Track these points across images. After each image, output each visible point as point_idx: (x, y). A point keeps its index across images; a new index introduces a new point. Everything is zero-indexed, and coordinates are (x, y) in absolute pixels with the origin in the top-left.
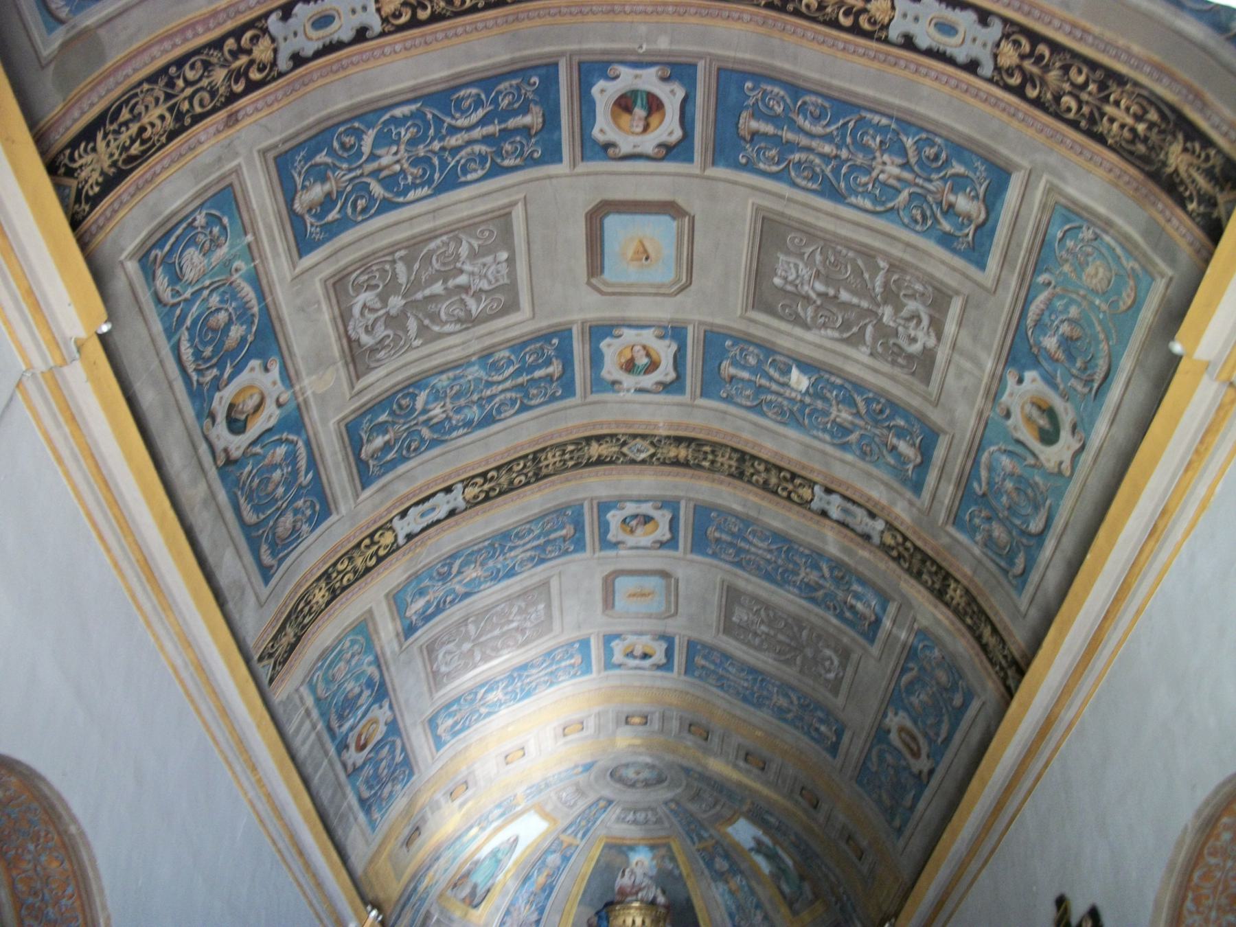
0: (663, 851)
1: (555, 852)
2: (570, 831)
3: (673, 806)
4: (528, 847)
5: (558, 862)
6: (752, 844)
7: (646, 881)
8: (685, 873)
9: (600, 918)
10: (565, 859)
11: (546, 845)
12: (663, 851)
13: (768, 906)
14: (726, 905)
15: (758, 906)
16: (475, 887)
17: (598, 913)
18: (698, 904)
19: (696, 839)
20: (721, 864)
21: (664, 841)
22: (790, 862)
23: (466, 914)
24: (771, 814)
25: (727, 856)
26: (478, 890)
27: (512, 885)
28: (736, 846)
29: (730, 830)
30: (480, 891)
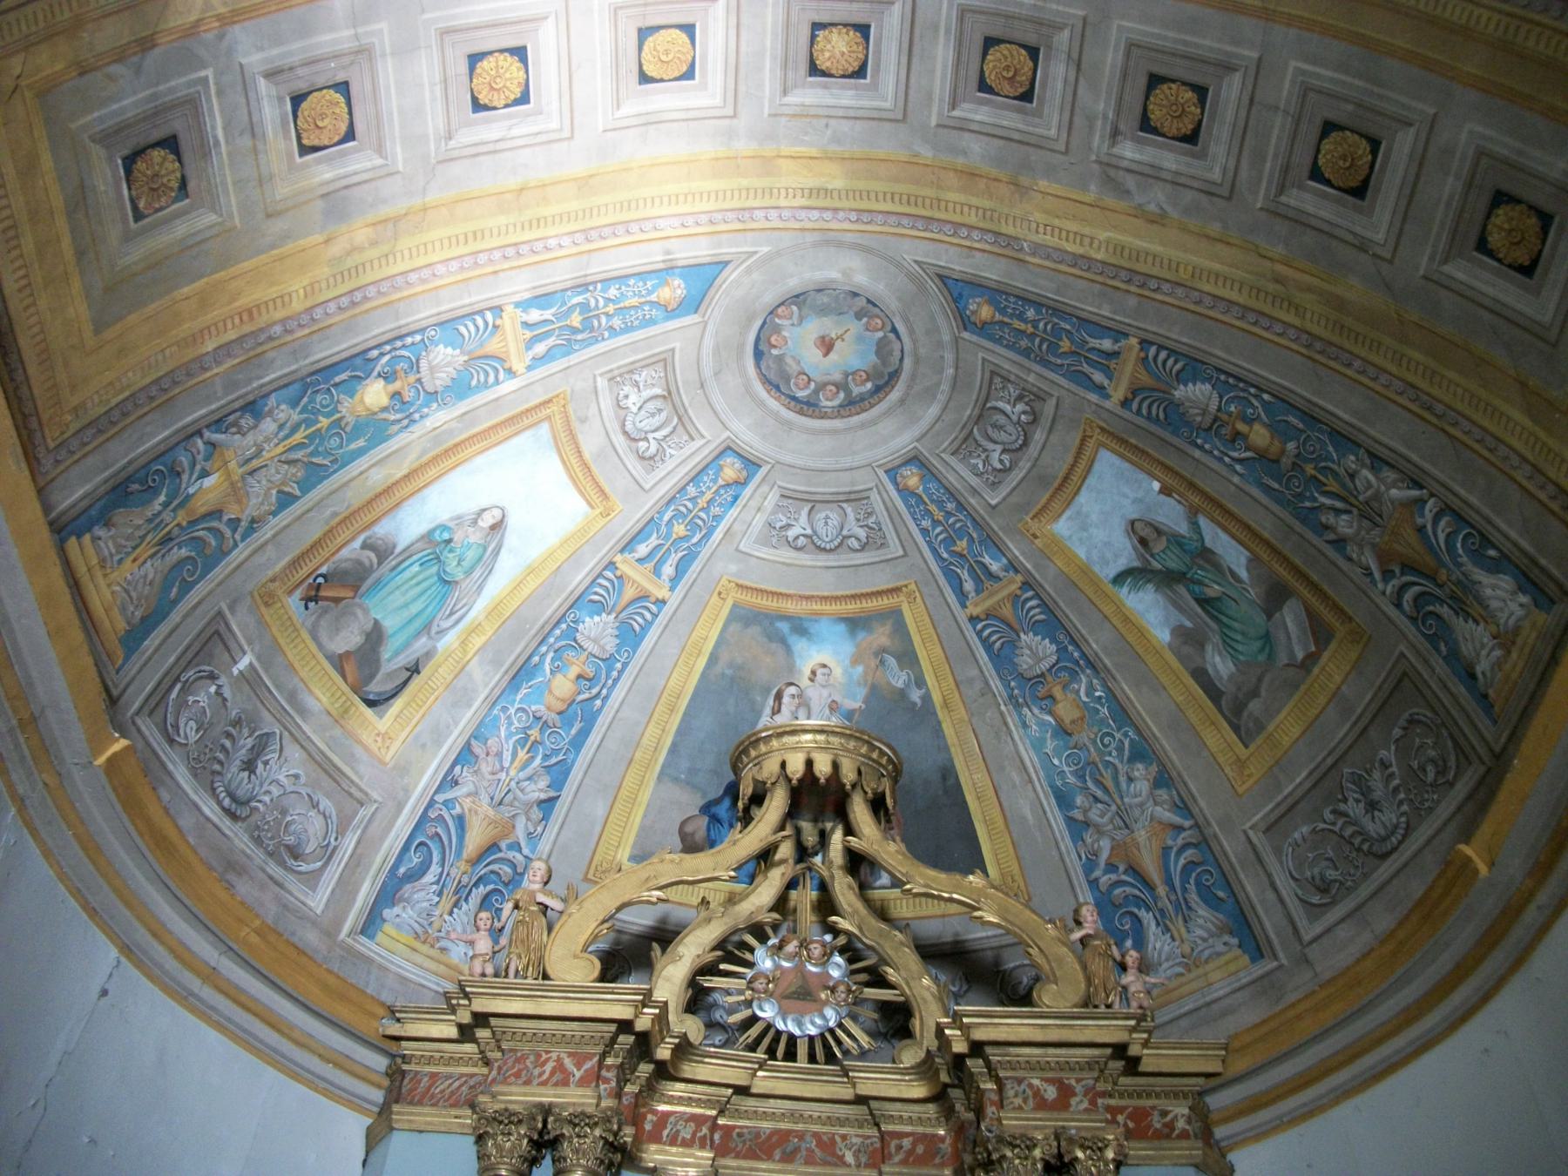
0: (881, 636)
1: (599, 607)
2: (642, 550)
3: (912, 479)
4: (531, 571)
5: (610, 644)
6: (1124, 554)
8: (936, 698)
9: (715, 819)
10: (630, 637)
11: (578, 578)
12: (881, 636)
13: (1167, 745)
15: (1142, 752)
17: (706, 809)
18: (973, 781)
19: (969, 586)
20: (1037, 651)
21: (885, 602)
22: (1234, 556)
24: (1195, 368)
25: (1053, 625)
26: (386, 654)
27: (484, 680)
28: (1079, 580)
29: (1062, 527)
30: (392, 659)
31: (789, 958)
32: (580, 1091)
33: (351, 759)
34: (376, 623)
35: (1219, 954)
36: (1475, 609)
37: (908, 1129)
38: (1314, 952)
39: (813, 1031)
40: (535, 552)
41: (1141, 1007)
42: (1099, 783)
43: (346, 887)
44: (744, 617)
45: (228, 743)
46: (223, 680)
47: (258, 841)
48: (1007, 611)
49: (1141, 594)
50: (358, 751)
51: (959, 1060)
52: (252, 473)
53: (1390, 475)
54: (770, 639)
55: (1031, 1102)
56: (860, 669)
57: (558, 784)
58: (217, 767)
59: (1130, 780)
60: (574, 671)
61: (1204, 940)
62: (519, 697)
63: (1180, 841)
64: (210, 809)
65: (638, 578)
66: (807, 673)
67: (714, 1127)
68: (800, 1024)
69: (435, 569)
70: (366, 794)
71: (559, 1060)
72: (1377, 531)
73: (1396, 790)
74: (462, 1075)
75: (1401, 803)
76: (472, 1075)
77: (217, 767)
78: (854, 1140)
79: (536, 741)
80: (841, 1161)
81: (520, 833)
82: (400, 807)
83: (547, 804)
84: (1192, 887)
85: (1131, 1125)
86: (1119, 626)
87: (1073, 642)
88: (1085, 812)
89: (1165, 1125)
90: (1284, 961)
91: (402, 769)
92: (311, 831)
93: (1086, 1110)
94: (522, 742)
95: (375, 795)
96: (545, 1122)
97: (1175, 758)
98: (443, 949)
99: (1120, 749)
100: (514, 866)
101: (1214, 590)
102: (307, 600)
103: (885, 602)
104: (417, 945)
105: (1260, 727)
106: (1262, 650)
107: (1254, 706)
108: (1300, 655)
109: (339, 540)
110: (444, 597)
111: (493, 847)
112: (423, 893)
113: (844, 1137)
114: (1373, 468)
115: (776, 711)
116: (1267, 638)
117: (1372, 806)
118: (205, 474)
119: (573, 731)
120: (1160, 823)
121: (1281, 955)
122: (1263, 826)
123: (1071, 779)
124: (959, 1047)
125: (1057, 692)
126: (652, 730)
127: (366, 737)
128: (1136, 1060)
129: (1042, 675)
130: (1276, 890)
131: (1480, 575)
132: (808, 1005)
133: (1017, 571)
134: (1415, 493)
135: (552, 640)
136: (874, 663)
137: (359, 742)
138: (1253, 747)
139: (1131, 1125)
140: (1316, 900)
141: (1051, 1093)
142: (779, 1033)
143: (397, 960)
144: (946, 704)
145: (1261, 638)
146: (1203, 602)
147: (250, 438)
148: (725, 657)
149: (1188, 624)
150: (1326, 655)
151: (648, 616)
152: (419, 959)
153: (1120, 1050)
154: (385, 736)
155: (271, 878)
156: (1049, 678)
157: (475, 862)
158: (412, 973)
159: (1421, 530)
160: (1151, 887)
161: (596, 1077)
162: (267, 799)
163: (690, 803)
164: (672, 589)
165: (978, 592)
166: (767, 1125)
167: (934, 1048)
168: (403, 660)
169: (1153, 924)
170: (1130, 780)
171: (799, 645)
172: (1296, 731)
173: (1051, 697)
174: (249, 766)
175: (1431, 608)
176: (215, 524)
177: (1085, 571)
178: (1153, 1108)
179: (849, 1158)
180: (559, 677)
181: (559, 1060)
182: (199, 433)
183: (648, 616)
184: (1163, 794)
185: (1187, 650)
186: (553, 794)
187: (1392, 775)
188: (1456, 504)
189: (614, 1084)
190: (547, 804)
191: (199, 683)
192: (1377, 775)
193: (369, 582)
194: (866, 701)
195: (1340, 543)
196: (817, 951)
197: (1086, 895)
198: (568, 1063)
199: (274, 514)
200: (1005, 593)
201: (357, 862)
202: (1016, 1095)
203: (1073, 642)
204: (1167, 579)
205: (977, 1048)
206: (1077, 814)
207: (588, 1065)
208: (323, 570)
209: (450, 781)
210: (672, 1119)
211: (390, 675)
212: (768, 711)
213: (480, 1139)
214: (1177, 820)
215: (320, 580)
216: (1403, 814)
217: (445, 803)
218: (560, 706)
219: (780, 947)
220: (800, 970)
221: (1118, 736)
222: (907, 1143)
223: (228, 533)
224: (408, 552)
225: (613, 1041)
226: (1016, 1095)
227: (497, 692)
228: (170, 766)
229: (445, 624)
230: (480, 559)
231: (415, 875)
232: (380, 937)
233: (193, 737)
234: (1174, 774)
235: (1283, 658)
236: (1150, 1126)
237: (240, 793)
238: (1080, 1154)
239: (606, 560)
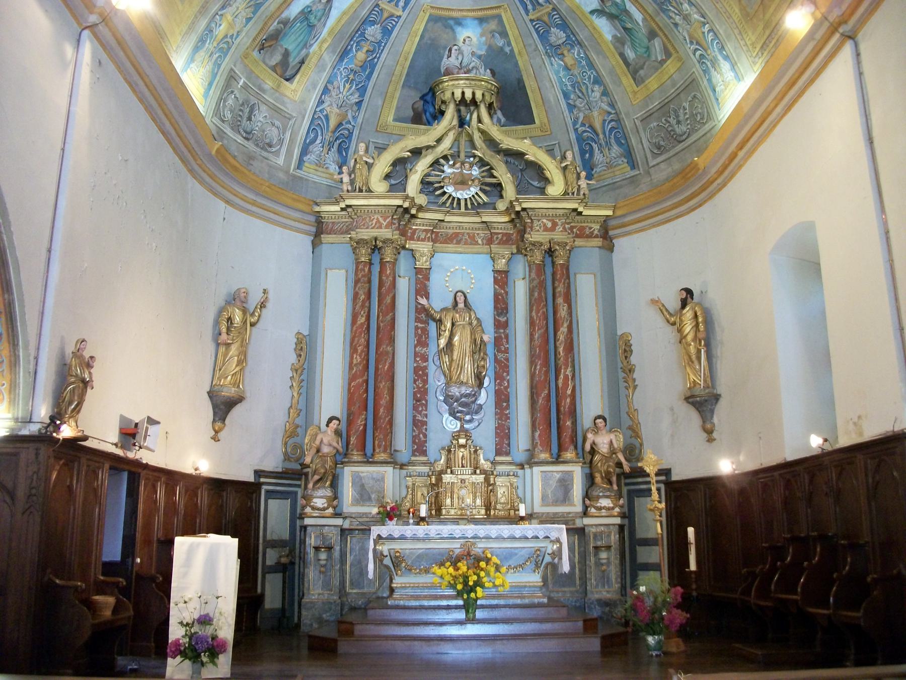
1: (373, 23)
4: (344, 13)
5: (379, 37)
7: (476, 62)
9: (426, 102)
10: (387, 32)
11: (364, 12)
12: (493, 25)
13: (607, 80)
14: (561, 82)
15: (598, 81)
16: (286, 54)
18: (530, 85)
19: (530, 7)
20: (557, 36)
21: (495, 12)
23: (279, 86)
25: (564, 26)
26: (291, 59)
27: (329, 60)
30: (293, 61)
31: (457, 169)
32: (386, 230)
33: (283, 103)
34: (286, 49)
35: (620, 165)
36: (718, 69)
37: (501, 231)
38: (652, 171)
39: (466, 197)
40: (345, 6)
41: (584, 194)
42: (581, 91)
43: (289, 153)
44: (433, 19)
45: (241, 113)
46: (236, 92)
47: (257, 145)
48: (546, 18)
49: (601, 20)
50: (286, 99)
51: (518, 213)
52: (236, 17)
53: (695, 10)
54: (446, 27)
55: (542, 228)
56: (484, 39)
57: (362, 95)
58: (239, 123)
59: (593, 91)
60: (365, 50)
61: (615, 158)
62: (344, 63)
63: (610, 118)
64: (240, 140)
65: (389, 9)
66: (462, 40)
67: (432, 232)
68: (462, 195)
69: (306, 23)
70: (290, 115)
71: (377, 219)
72: (688, 26)
73: (687, 119)
74: (343, 222)
75: (688, 124)
76: (347, 222)
77: (239, 123)
78: (482, 235)
79: (352, 80)
80: (477, 243)
81: (350, 117)
82: (304, 117)
83: (359, 104)
84: (612, 137)
85: (578, 232)
86: (592, 31)
87: (573, 33)
88: (575, 101)
89: (590, 232)
90: (642, 172)
91: (303, 102)
92: (274, 135)
93: (561, 231)
94: (347, 81)
95: (294, 115)
96: (376, 242)
97: (611, 87)
98: (327, 168)
99: (589, 78)
100: (349, 130)
101: (629, 26)
102: (260, 51)
103: (495, 12)
104: (317, 168)
105: (643, 81)
106: (646, 52)
107: (642, 72)
108: (659, 59)
109: (269, 25)
110: (310, 33)
111: (340, 124)
112: (316, 148)
113: (478, 234)
114: (689, 4)
115: (449, 56)
116: (648, 48)
117: (679, 122)
118: (220, 25)
119: (367, 73)
120: (603, 109)
121: (641, 169)
122: (640, 119)
123: (570, 88)
124: (518, 209)
125: (565, 52)
126: (399, 68)
127: (288, 93)
128: (582, 212)
129: (559, 45)
130: (642, 144)
131: (720, 57)
132: (465, 187)
133: (550, 3)
134: (702, 19)
135: (355, 39)
136: (490, 36)
137: (286, 96)
138: (639, 88)
139: (578, 232)
140: (655, 151)
141: (549, 225)
142: (454, 198)
143: (311, 175)
144: (520, 53)
145: (645, 48)
146: (625, 29)
147: (234, 6)
148: (427, 36)
149: (619, 35)
150: (669, 62)
151: (394, 23)
152: (319, 174)
153: (575, 210)
154: (294, 91)
155: (264, 157)
156: (562, 47)
157: (334, 132)
158: (317, 179)
159: (704, 33)
160: (598, 135)
161: (391, 224)
162: (257, 128)
163: (415, 96)
164: (403, 11)
165: (534, 10)
166: (451, 231)
167: (509, 206)
168: (298, 60)
169: (597, 149)
170: (593, 91)
171: (458, 29)
172: (656, 86)
173: (562, 54)
174: (249, 119)
175: (704, 61)
176: (226, 40)
177: (578, 7)
178: (587, 226)
179: (480, 242)
180: (359, 53)
181: (377, 219)
182: (217, 14)
183: (394, 23)
184: (605, 99)
185: (617, 44)
186: (361, 99)
187: (686, 113)
188: (715, 30)
189: (397, 225)
190: (359, 104)
191: (229, 96)
192: (681, 111)
193: (282, 34)
194: (487, 51)
195: (676, 25)
196: (467, 166)
197: (573, 136)
198: (380, 219)
199: (245, 27)
200: (544, 11)
201: (292, 141)
202: (537, 226)
203: (573, 33)
204: (612, 17)
205: (524, 209)
206: (570, 102)
207: (388, 220)
208: (264, 37)
209: (321, 102)
210: (417, 231)
211: (293, 67)
212: (446, 56)
213: (354, 249)
214: (609, 110)
215: (264, 41)
216: (688, 129)
217: (320, 111)
218: (361, 64)
219: (454, 164)
220: (461, 174)
221: (589, 73)
222: (500, 236)
223: (230, 40)
224: (296, 19)
225: (396, 211)
226: (537, 226)
227: (335, 63)
228: (225, 130)
229: (312, 42)
230: (323, 14)
231: (313, 141)
232: (304, 168)
233: (230, 116)
234: (610, 92)
235: (653, 58)
236: (584, 233)
237: (248, 130)
238: (557, 248)
239: (375, 4)
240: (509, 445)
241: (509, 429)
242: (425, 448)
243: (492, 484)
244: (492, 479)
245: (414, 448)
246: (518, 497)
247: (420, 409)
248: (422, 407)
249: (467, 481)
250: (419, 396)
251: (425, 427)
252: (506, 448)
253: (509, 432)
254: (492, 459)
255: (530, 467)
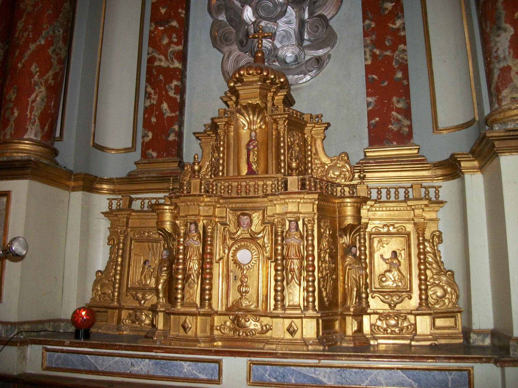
240: (407, 113)
241: (404, 68)
242: (172, 137)
243: (352, 227)
244: (349, 211)
245: (147, 139)
246: (441, 271)
247: (166, 41)
248: (170, 37)
249: (256, 217)
250: (163, 11)
251: (175, 83)
252: (398, 121)
253: (406, 76)
254: (356, 157)
255: (481, 169)
